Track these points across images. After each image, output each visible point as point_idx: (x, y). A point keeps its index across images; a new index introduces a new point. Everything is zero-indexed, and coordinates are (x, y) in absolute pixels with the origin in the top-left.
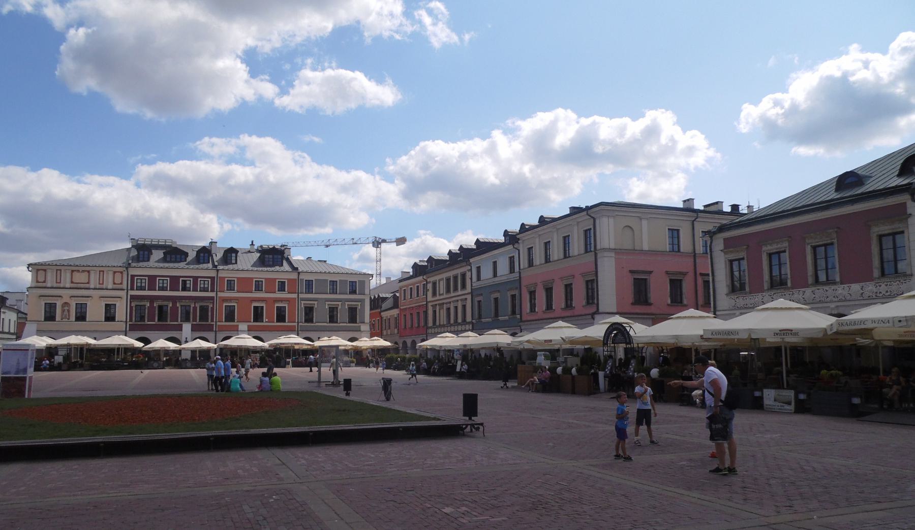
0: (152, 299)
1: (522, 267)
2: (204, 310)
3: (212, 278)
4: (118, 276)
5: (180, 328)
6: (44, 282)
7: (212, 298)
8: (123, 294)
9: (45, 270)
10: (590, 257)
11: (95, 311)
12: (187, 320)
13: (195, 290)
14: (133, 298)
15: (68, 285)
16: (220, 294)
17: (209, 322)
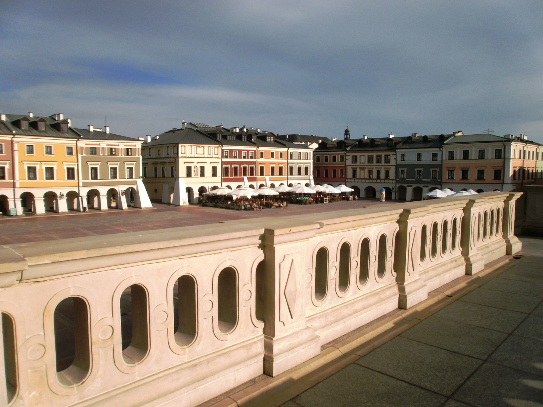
0: (231, 163)
1: (444, 158)
2: (252, 168)
3: (255, 151)
4: (216, 149)
5: (242, 180)
6: (185, 153)
7: (255, 162)
8: (219, 160)
9: (185, 146)
10: (500, 161)
11: (208, 171)
12: (245, 174)
13: (248, 158)
14: (224, 163)
15: (196, 156)
16: (259, 160)
17: (254, 176)
